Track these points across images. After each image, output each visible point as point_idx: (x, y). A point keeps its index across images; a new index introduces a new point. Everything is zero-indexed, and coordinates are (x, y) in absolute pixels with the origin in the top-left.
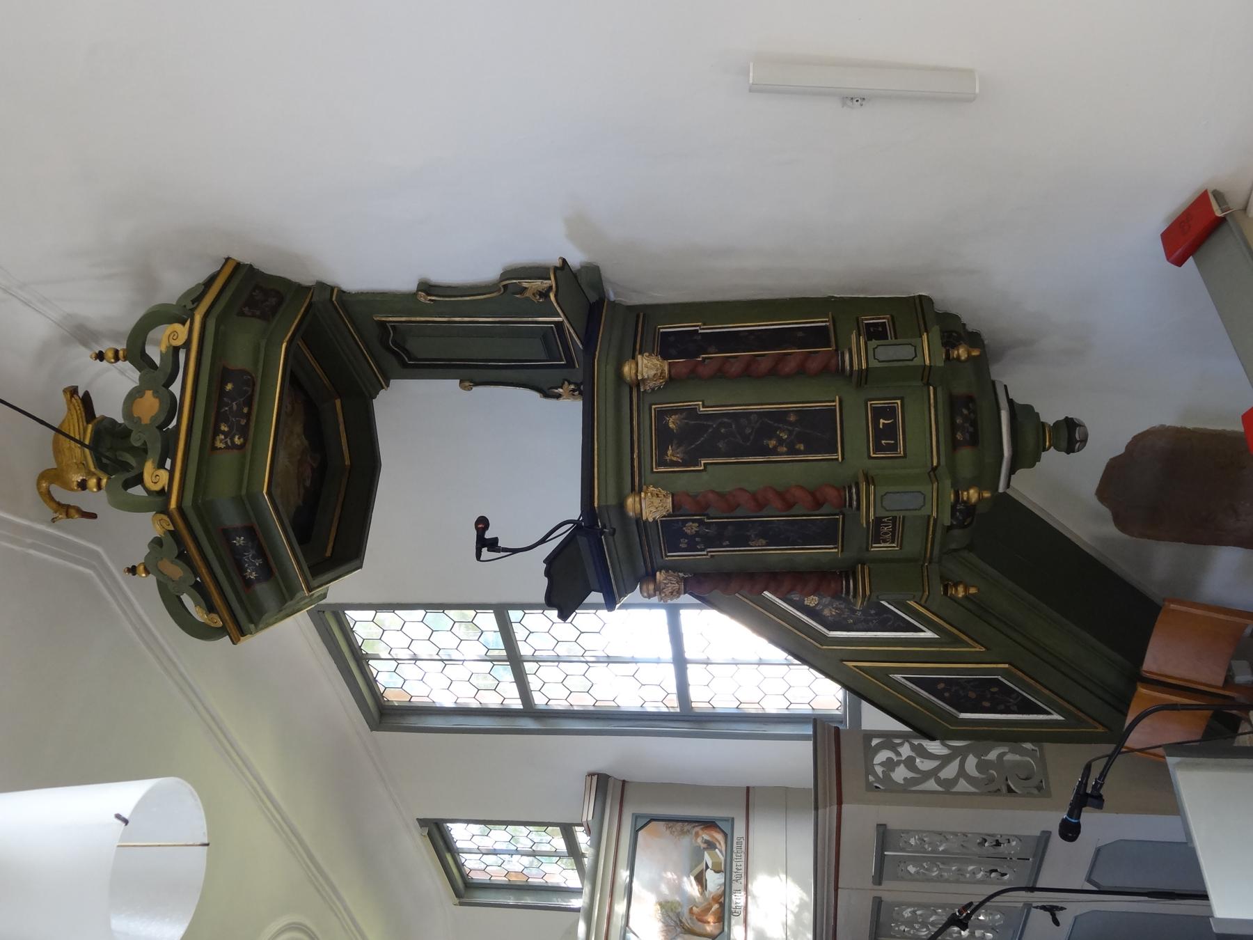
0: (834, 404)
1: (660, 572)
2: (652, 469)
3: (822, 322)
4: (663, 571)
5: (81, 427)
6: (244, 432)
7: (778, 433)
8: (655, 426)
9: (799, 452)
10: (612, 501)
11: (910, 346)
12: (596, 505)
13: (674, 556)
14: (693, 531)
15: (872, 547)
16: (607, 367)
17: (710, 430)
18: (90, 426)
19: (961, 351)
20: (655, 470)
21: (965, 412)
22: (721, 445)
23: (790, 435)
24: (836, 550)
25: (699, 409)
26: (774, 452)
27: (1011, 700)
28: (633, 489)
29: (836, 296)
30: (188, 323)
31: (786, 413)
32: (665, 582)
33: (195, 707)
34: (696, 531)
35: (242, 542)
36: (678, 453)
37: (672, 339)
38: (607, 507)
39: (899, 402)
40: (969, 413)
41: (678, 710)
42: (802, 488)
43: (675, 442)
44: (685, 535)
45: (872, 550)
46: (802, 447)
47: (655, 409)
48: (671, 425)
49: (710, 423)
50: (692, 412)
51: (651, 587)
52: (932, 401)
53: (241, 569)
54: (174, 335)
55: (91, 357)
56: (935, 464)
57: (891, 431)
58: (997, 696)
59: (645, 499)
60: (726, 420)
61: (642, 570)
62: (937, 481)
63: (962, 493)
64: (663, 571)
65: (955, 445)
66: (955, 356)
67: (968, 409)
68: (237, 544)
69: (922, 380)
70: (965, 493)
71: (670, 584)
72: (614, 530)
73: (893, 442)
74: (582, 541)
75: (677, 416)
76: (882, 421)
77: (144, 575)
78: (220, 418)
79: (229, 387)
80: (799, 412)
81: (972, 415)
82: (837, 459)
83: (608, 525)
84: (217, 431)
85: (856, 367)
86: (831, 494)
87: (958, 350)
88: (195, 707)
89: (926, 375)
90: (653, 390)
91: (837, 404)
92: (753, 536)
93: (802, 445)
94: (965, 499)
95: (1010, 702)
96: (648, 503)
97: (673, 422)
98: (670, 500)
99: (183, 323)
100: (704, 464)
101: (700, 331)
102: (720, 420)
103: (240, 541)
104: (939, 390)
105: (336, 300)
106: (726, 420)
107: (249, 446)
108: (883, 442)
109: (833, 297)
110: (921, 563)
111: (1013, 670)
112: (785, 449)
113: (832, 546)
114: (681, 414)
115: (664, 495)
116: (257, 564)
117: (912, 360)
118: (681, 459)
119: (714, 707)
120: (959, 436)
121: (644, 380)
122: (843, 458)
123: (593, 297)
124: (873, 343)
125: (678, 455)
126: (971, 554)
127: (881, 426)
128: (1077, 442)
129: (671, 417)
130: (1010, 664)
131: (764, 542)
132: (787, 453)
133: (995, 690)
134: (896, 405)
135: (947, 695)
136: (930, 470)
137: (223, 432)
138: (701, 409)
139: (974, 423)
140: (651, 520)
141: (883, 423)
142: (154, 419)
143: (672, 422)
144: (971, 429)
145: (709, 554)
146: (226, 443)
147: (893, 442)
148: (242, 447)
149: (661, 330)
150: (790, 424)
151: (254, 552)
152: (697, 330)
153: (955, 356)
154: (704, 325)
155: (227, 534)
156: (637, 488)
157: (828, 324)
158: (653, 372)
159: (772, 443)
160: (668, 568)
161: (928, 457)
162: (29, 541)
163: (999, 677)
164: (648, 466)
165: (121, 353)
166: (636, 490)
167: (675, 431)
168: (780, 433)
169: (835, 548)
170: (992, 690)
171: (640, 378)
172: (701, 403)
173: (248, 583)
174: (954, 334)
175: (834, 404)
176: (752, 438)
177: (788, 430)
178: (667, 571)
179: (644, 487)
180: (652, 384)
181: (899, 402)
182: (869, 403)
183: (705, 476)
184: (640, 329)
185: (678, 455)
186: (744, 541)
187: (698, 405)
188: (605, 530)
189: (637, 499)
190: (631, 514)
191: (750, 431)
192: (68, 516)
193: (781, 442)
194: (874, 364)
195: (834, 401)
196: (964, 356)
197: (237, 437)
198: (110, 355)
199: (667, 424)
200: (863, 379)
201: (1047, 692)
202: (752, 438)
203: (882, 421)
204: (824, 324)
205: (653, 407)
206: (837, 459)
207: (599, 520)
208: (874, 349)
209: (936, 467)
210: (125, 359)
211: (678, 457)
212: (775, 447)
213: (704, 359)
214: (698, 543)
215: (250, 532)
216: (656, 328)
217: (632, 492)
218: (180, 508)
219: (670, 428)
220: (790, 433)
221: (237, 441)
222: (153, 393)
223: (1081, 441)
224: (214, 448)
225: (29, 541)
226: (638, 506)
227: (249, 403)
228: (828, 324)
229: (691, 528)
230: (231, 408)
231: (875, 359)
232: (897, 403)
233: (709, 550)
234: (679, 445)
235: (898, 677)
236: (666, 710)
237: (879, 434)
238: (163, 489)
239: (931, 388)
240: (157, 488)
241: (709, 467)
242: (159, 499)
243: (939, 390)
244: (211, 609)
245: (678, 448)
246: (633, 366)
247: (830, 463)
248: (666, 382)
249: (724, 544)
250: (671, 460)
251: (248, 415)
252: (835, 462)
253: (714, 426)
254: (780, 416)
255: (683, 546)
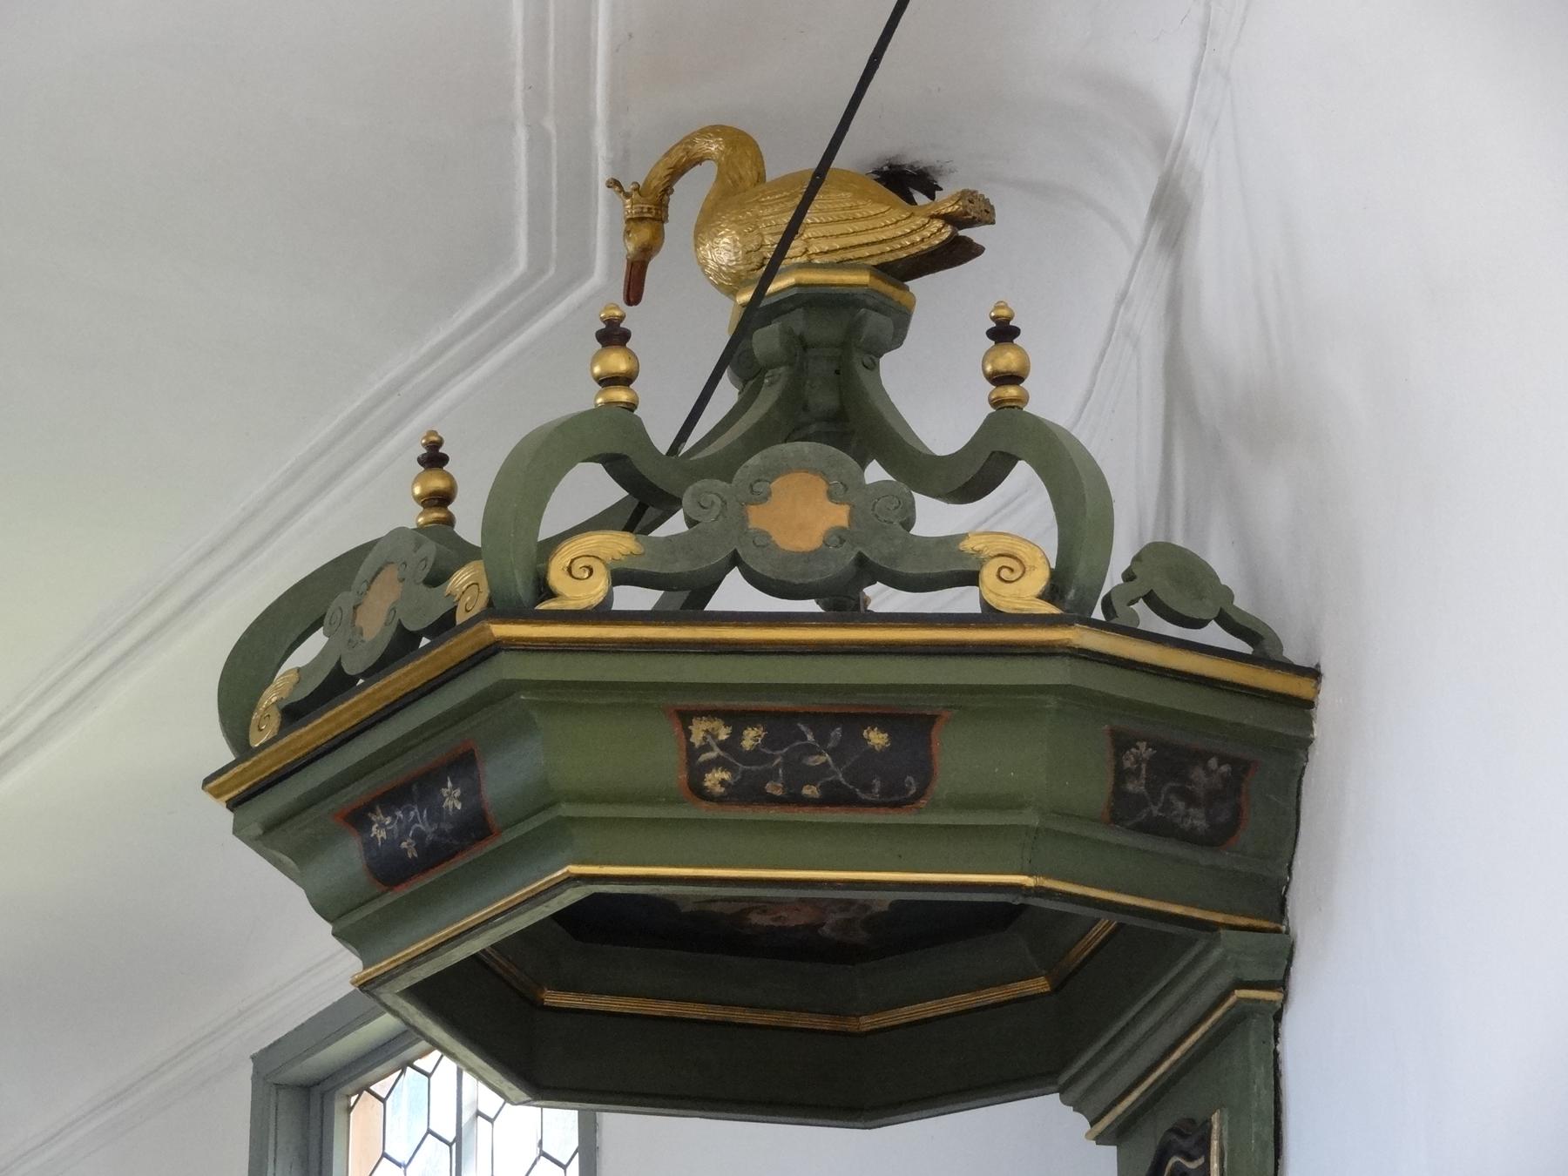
5: (866, 252)
6: (746, 792)
18: (864, 278)
30: (1053, 610)
33: (212, 551)
35: (450, 803)
53: (392, 799)
54: (1012, 570)
55: (997, 307)
68: (445, 792)
77: (417, 491)
78: (780, 723)
79: (877, 738)
84: (737, 719)
88: (212, 551)
99: (1042, 596)
103: (452, 799)
105: (1240, 1000)
107: (704, 811)
116: (404, 845)
137: (736, 736)
142: (764, 542)
146: (706, 748)
148: (698, 791)
151: (430, 837)
155: (463, 764)
162: (550, 125)
165: (1011, 391)
173: (358, 819)
192: (636, 220)
197: (726, 776)
198: (1007, 360)
210: (997, 403)
215: (475, 827)
218: (495, 648)
221: (715, 779)
222: (843, 529)
224: (686, 717)
225: (550, 125)
227: (834, 797)
230: (811, 750)
238: (551, 594)
240: (556, 577)
242: (521, 587)
244: (293, 714)
251: (794, 799)
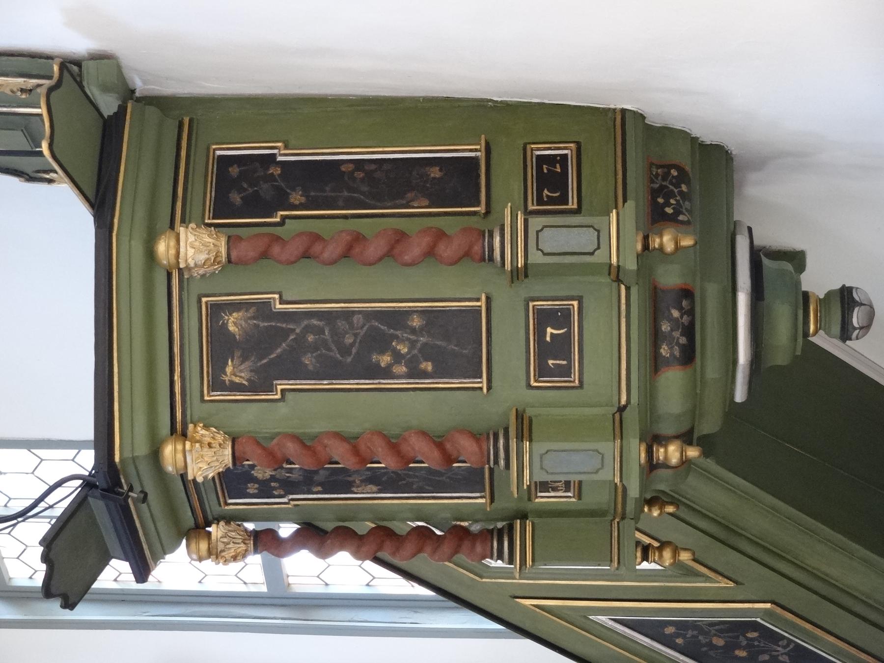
0: (478, 304)
1: (218, 524)
2: (202, 395)
3: (471, 150)
4: (222, 523)
7: (394, 344)
8: (207, 328)
9: (424, 375)
10: (142, 449)
11: (591, 229)
12: (117, 459)
13: (236, 504)
14: (267, 474)
15: (537, 497)
16: (133, 242)
17: (292, 337)
19: (666, 238)
20: (206, 398)
21: (676, 314)
22: (308, 360)
23: (411, 348)
24: (482, 501)
25: (275, 305)
26: (387, 373)
27: (779, 649)
28: (173, 430)
29: (495, 99)
31: (408, 313)
32: (225, 540)
34: (271, 475)
36: (241, 371)
37: (234, 171)
38: (134, 459)
39: (575, 303)
40: (682, 317)
41: (264, 589)
42: (424, 434)
43: (237, 354)
44: (255, 480)
45: (537, 500)
46: (428, 366)
47: (206, 303)
48: (232, 328)
49: (291, 326)
50: (263, 309)
51: (204, 546)
52: (623, 307)
56: (623, 401)
57: (561, 347)
58: (756, 643)
59: (191, 451)
60: (315, 322)
61: (189, 521)
62: (622, 439)
63: (658, 451)
64: (222, 523)
65: (656, 364)
66: (657, 246)
67: (680, 309)
69: (609, 274)
70: (662, 450)
71: (231, 545)
72: (146, 495)
73: (564, 362)
74: (98, 506)
75: (240, 314)
76: (549, 330)
80: (423, 312)
81: (685, 317)
82: (481, 389)
83: (137, 488)
85: (508, 266)
86: (467, 446)
87: (661, 237)
89: (617, 275)
90: (203, 276)
91: (482, 303)
92: (358, 482)
93: (430, 363)
94: (661, 458)
95: (778, 651)
96: (195, 455)
97: (235, 324)
98: (228, 451)
100: (282, 390)
101: (280, 159)
102: (306, 322)
104: (634, 291)
106: (315, 322)
108: (550, 362)
109: (491, 100)
110: (611, 518)
111: (779, 610)
112: (404, 369)
113: (478, 495)
114: (247, 311)
115: (220, 445)
117: (592, 254)
118: (246, 381)
119: (327, 584)
120: (664, 351)
121: (188, 268)
122: (489, 388)
123: (109, 105)
124: (536, 223)
125: (243, 375)
126: (708, 460)
127: (548, 339)
128: (855, 329)
129: (231, 314)
130: (773, 602)
131: (375, 488)
132: (410, 375)
133: (752, 635)
134: (571, 307)
135: (679, 641)
136: (616, 409)
138: (278, 306)
139: (689, 331)
140: (200, 479)
141: (552, 334)
143: (234, 323)
144: (683, 340)
145: (292, 503)
147: (564, 362)
149: (219, 153)
150: (413, 331)
152: (274, 155)
153: (657, 246)
154: (286, 147)
156: (179, 426)
157: (478, 154)
158: (202, 257)
159: (385, 360)
160: (229, 519)
161: (615, 392)
163: (758, 620)
164: (196, 394)
166: (179, 432)
167: (238, 337)
168: (397, 345)
169: (481, 497)
170: (749, 635)
171: (182, 266)
172: (277, 296)
174: (674, 173)
175: (478, 304)
176: (354, 350)
177: (408, 339)
178: (228, 522)
179: (191, 426)
180: (201, 272)
181: (575, 303)
182: (531, 304)
183: (283, 409)
184: (183, 153)
185: (243, 375)
186: (347, 487)
187: (274, 299)
188: (131, 494)
189: (179, 447)
190: (170, 469)
191: (351, 341)
193: (398, 357)
194: (536, 257)
195: (478, 300)
196: (669, 247)
199: (225, 326)
200: (520, 275)
201: (831, 639)
202: (354, 350)
203: (549, 330)
204: (473, 154)
205: (204, 300)
206: (481, 389)
207: (122, 477)
208: (538, 232)
209: (625, 407)
211: (241, 377)
212: (389, 366)
213: (284, 218)
214: (275, 488)
216: (208, 149)
217: (172, 434)
219: (229, 330)
220: (413, 344)
223: (861, 328)
226: (180, 456)
228: (478, 154)
229: (262, 473)
231: (538, 249)
232: (573, 305)
233: (291, 497)
234: (244, 359)
235: (603, 619)
236: (242, 588)
237: (545, 350)
239: (623, 287)
241: (289, 396)
243: (634, 291)
245: (242, 362)
246: (172, 243)
247: (470, 393)
248: (223, 267)
249: (315, 489)
250: (231, 382)
252: (478, 392)
253: (298, 331)
254: (397, 319)
255: (251, 491)
